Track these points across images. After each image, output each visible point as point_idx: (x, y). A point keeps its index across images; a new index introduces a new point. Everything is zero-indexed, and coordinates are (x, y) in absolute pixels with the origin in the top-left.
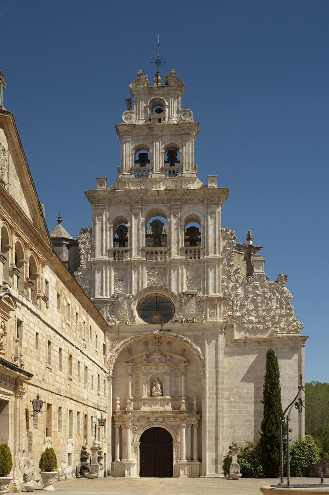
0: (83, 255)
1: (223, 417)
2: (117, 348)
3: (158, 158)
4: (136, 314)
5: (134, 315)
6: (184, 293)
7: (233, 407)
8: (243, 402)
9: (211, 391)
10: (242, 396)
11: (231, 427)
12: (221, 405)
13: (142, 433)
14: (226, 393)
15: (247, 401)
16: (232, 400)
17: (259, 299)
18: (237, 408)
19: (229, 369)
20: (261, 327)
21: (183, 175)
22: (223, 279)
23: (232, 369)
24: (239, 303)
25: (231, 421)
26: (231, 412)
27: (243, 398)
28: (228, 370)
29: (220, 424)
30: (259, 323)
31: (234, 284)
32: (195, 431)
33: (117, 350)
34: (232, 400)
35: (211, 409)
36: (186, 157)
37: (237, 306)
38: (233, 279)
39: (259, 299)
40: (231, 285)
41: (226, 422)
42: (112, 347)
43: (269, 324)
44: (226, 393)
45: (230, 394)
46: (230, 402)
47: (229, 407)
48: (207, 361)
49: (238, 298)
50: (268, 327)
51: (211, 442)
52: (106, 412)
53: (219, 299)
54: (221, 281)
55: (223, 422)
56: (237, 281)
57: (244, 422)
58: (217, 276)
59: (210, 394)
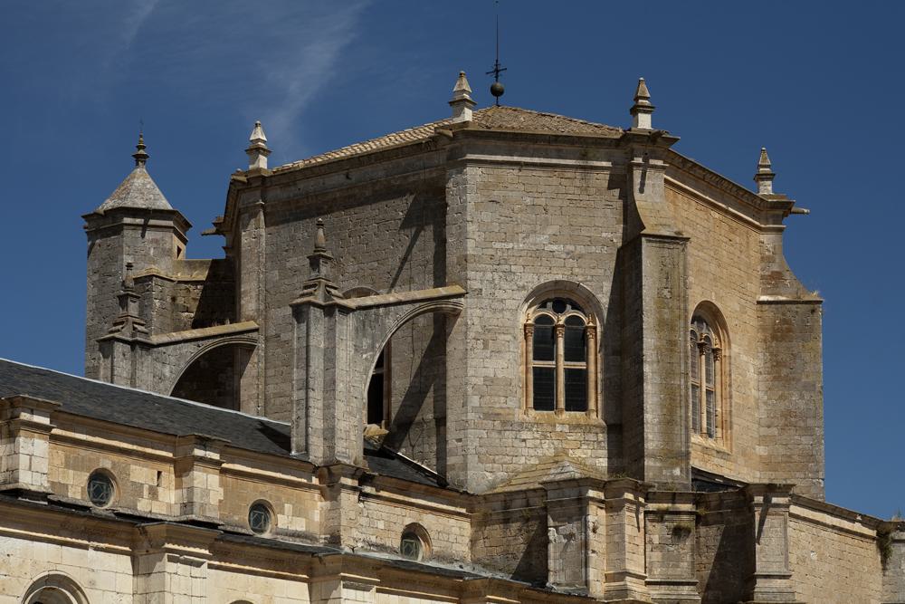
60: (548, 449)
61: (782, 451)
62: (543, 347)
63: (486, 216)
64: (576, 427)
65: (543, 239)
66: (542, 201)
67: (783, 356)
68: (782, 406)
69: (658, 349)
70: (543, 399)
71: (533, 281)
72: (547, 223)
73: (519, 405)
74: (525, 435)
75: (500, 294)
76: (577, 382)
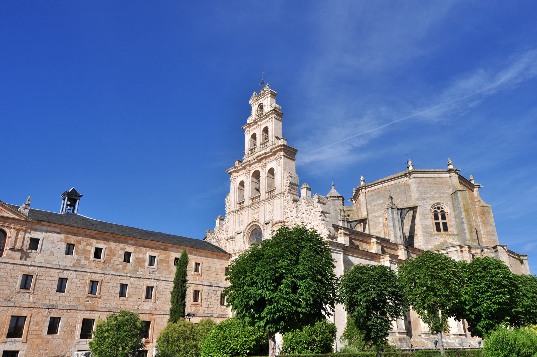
3: (260, 139)
39: (304, 215)
40: (288, 211)
60: (442, 240)
61: (488, 240)
62: (436, 218)
63: (420, 189)
64: (447, 235)
65: (433, 193)
66: (432, 185)
67: (484, 219)
68: (486, 230)
69: (466, 216)
70: (438, 229)
71: (432, 203)
72: (433, 190)
73: (434, 230)
74: (436, 237)
75: (425, 206)
76: (445, 225)
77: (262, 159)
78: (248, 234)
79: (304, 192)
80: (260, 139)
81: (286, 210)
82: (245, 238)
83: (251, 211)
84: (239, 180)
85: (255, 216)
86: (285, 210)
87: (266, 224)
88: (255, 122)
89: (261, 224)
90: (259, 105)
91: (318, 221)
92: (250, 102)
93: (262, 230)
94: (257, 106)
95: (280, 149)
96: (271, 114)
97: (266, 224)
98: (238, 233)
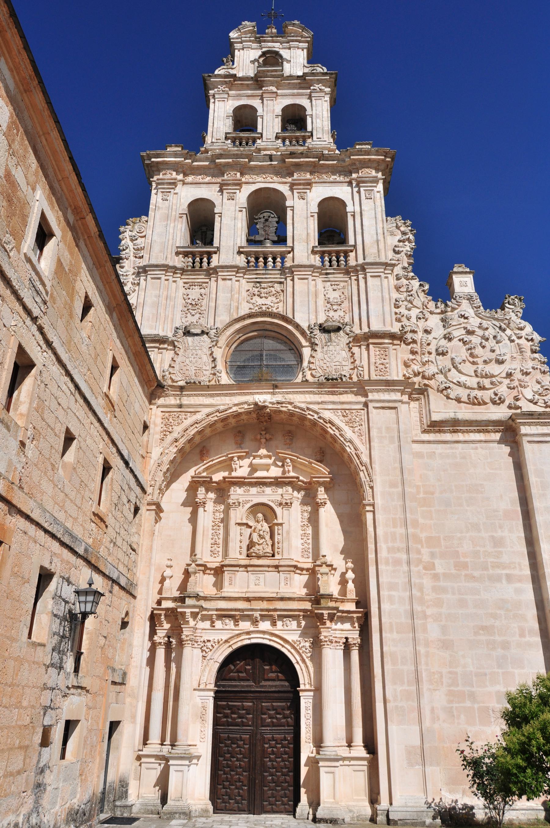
0: (127, 259)
1: (425, 617)
2: (175, 435)
3: (269, 124)
4: (220, 366)
5: (218, 368)
6: (320, 326)
7: (444, 590)
8: (466, 575)
9: (390, 545)
10: (462, 559)
11: (446, 645)
12: (417, 581)
13: (221, 659)
14: (425, 551)
15: (476, 574)
16: (439, 569)
17: (475, 340)
18: (454, 594)
19: (425, 493)
20: (487, 395)
21: (313, 143)
22: (396, 301)
23: (433, 493)
24: (432, 348)
25: (444, 629)
26: (439, 603)
27: (465, 566)
28: (421, 495)
29: (420, 635)
30: (481, 388)
31: (419, 311)
32: (355, 655)
33: (176, 440)
34: (439, 569)
35: (393, 593)
36: (318, 120)
37: (430, 353)
38: (417, 302)
39: (475, 340)
40: (414, 313)
41: (433, 631)
42: (166, 433)
43: (503, 390)
44: (425, 551)
45: (432, 555)
46: (436, 577)
47: (434, 589)
48: (377, 466)
49: (430, 337)
50: (500, 399)
51: (399, 688)
52: (134, 597)
53: (392, 336)
54: (393, 306)
55: (425, 630)
56: (425, 306)
57: (476, 634)
58: (386, 296)
59: (390, 550)
77: (298, 167)
78: (229, 345)
79: (463, 283)
80: (269, 124)
81: (402, 310)
82: (218, 353)
83: (244, 284)
84: (187, 194)
85: (260, 301)
86: (397, 311)
87: (324, 329)
88: (257, 82)
89: (297, 326)
90: (264, 54)
91: (530, 364)
92: (233, 35)
93: (304, 342)
94: (259, 53)
95: (378, 162)
96: (319, 82)
97: (324, 329)
98: (187, 333)
